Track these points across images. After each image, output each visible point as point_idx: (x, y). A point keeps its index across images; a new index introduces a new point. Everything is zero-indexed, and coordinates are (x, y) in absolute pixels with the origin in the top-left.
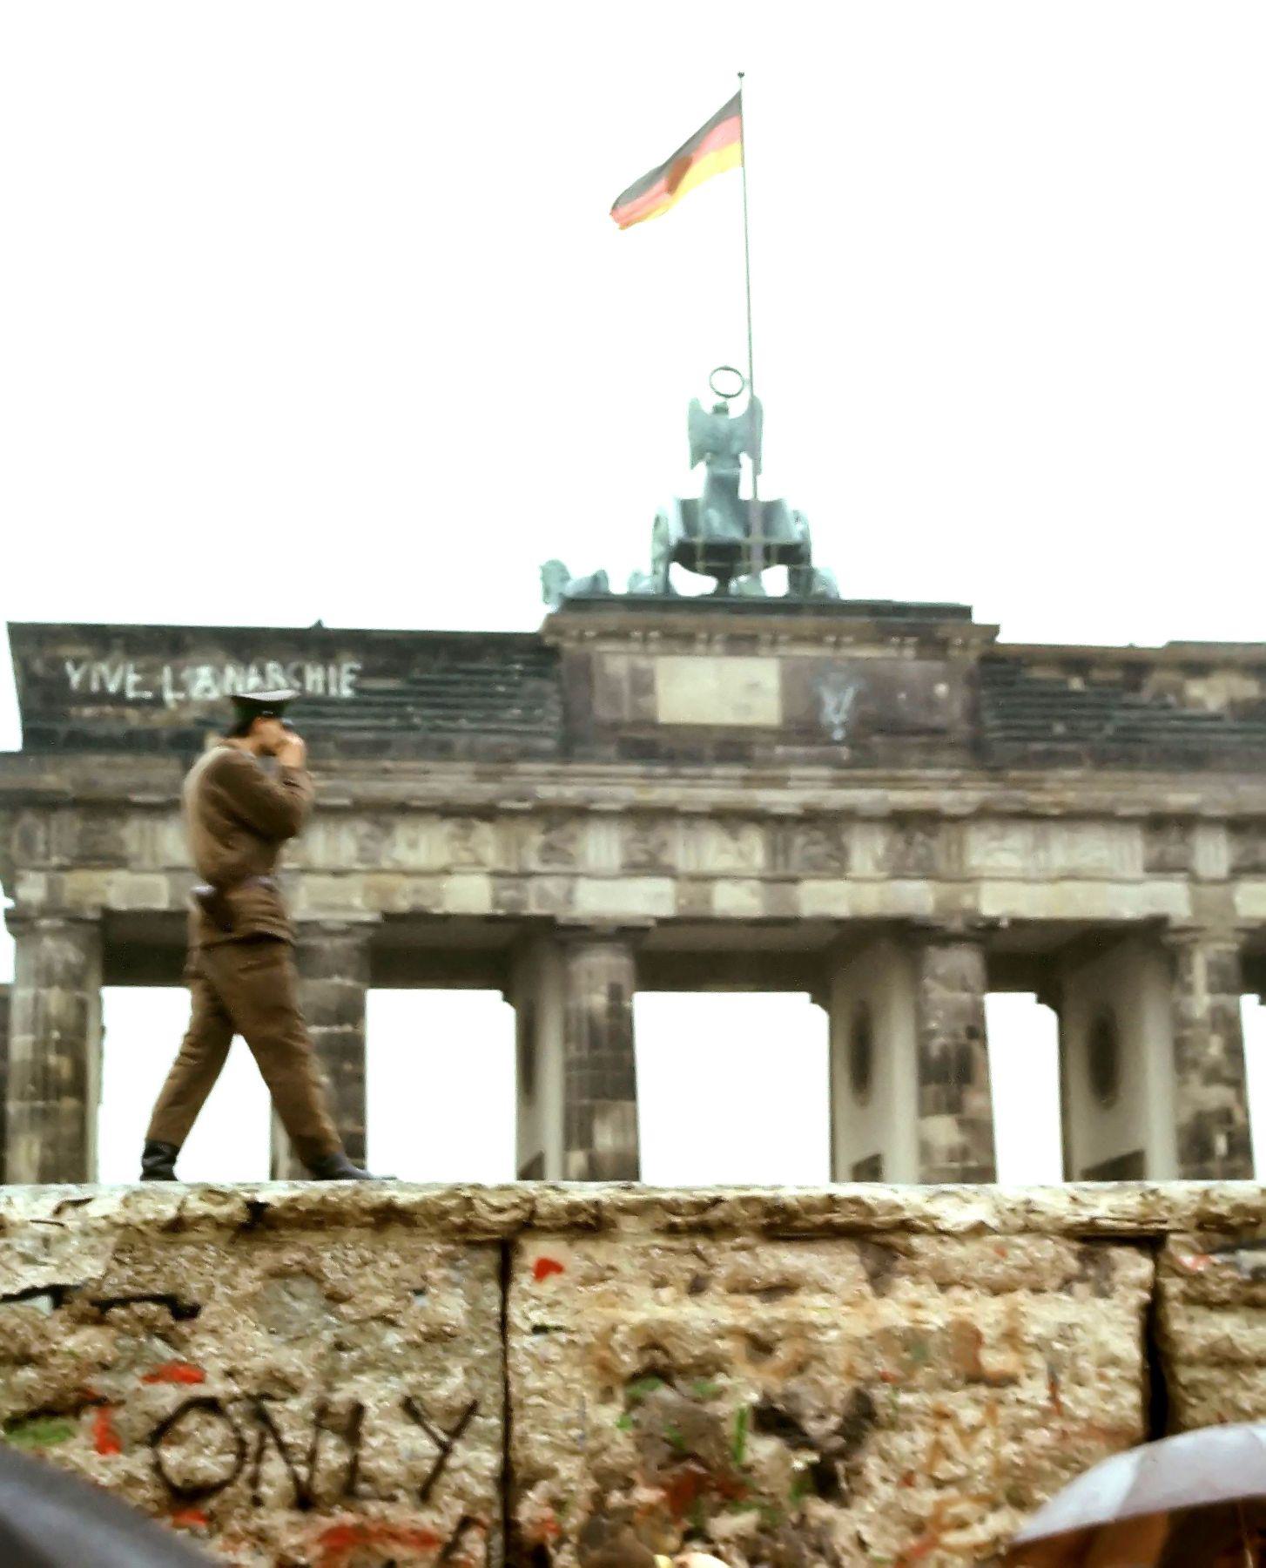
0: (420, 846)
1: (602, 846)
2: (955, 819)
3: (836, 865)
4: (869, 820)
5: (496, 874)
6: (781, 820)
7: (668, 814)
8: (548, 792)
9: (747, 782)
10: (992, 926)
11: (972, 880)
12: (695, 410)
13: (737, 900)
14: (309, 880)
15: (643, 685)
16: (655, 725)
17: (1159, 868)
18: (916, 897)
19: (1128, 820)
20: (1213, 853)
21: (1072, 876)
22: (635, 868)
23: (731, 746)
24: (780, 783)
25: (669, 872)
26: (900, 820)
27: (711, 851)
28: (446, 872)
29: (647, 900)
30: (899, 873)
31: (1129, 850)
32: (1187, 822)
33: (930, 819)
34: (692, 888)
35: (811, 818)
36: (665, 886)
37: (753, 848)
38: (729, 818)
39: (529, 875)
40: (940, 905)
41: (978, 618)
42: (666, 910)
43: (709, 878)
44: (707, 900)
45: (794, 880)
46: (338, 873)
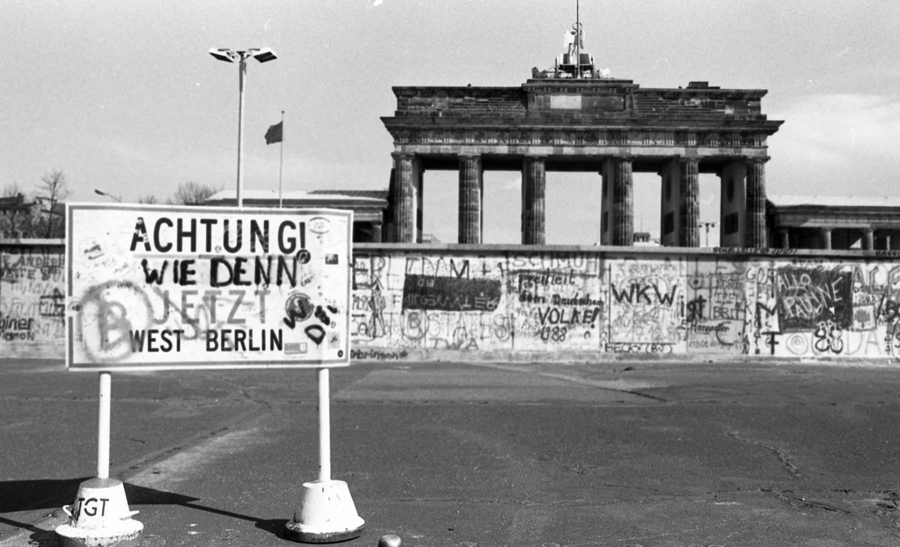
2: (624, 132)
4: (602, 132)
6: (580, 132)
7: (552, 130)
13: (568, 151)
14: (463, 147)
16: (549, 109)
18: (614, 151)
19: (670, 132)
22: (542, 145)
23: (569, 115)
26: (610, 132)
28: (497, 144)
29: (547, 151)
32: (686, 132)
34: (559, 148)
35: (587, 131)
36: (551, 148)
39: (517, 145)
40: (620, 152)
42: (551, 153)
44: (562, 151)
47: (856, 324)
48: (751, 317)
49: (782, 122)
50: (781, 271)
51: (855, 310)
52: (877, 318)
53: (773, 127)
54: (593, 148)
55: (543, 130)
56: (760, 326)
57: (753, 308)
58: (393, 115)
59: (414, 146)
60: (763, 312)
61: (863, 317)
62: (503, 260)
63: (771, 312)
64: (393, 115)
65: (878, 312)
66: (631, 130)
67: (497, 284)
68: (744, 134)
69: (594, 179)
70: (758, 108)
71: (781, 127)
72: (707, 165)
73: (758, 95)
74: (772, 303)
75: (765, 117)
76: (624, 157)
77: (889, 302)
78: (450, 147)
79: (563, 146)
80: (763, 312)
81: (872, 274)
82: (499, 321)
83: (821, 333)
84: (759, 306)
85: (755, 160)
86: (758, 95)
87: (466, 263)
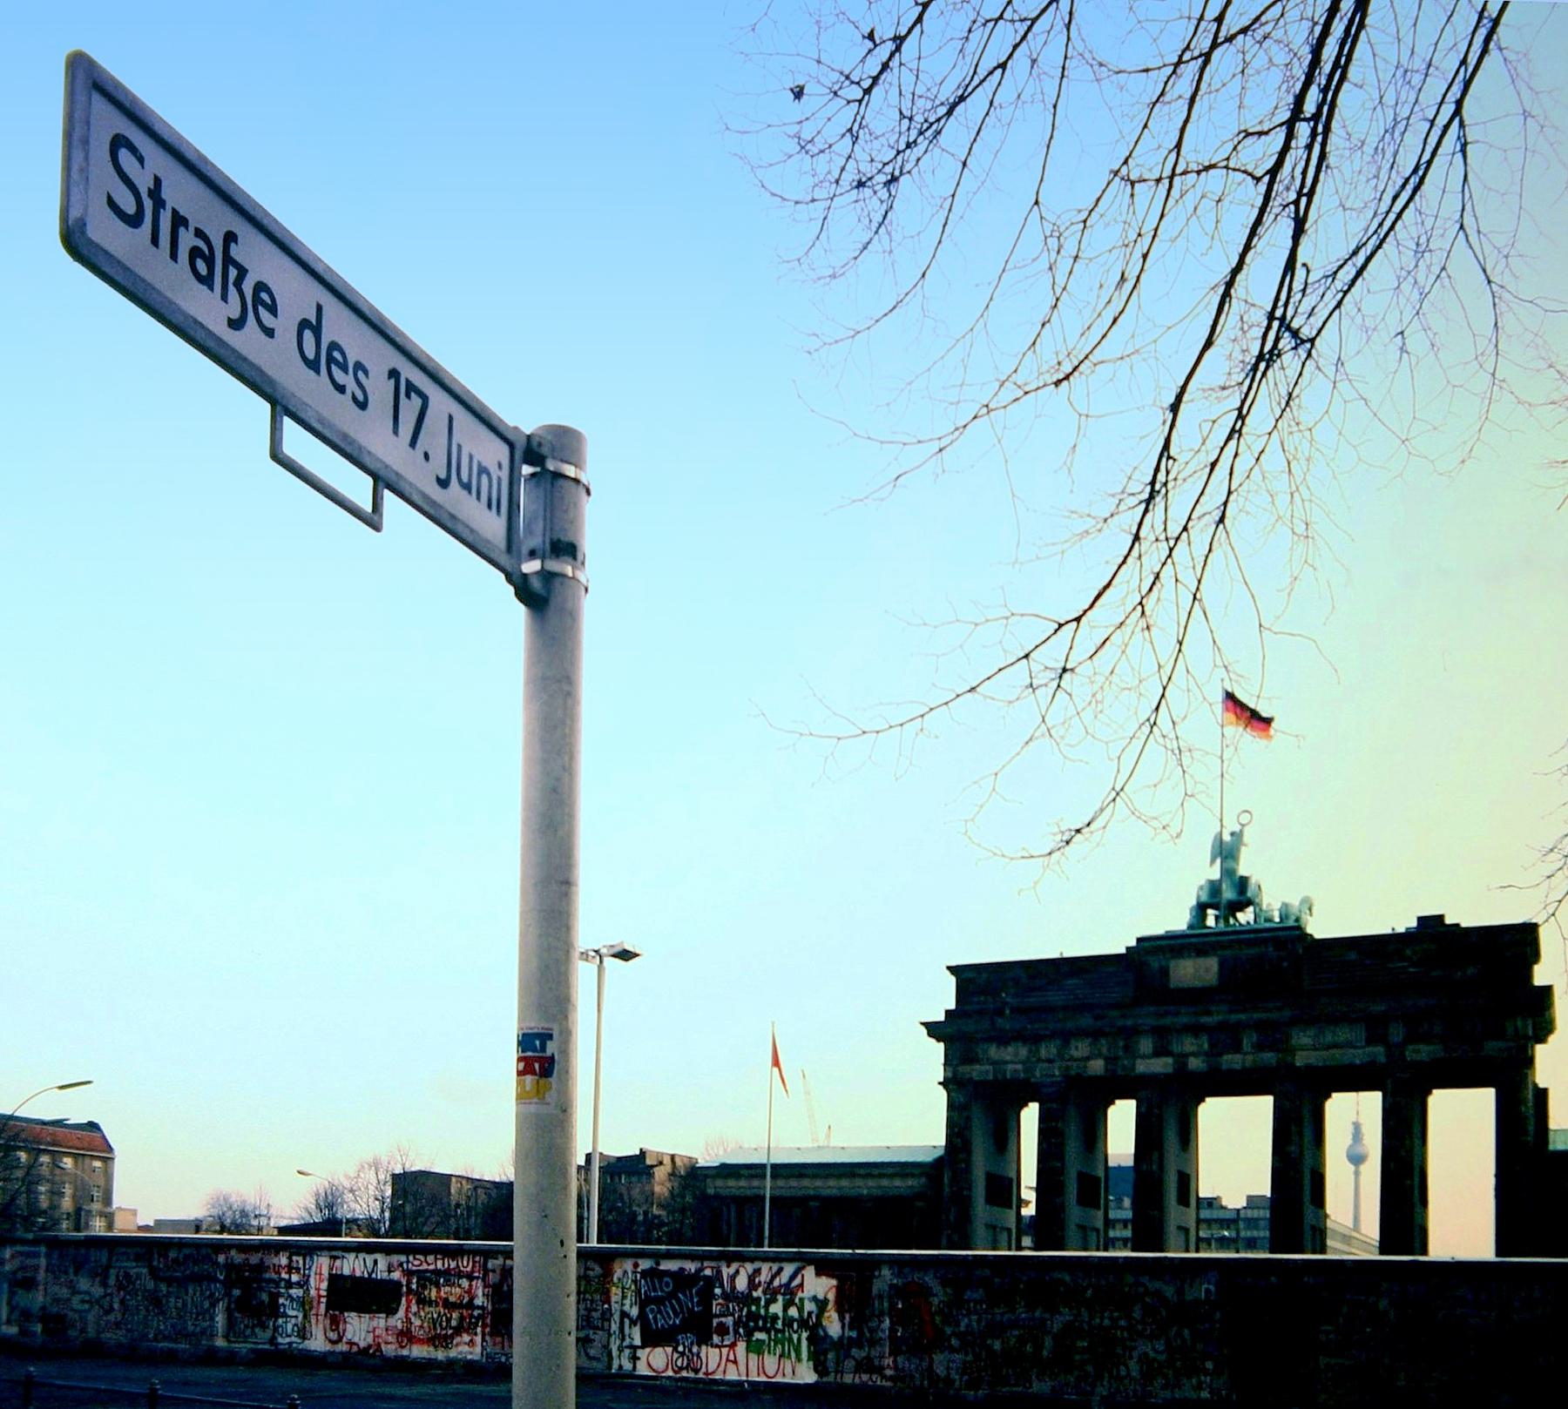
0: (1080, 1048)
1: (1146, 1045)
3: (1237, 1048)
5: (1106, 1059)
8: (1120, 1023)
9: (1196, 1014)
11: (1292, 1051)
13: (1195, 1063)
15: (1165, 972)
17: (1370, 1041)
18: (1269, 1057)
20: (1397, 1033)
21: (1336, 1046)
24: (1209, 1013)
25: (1168, 1053)
27: (1188, 1044)
28: (1088, 1058)
30: (1260, 1047)
35: (1222, 1026)
36: (1170, 1060)
38: (1195, 1030)
43: (1186, 1056)
44: (1185, 1064)
45: (1221, 1055)
46: (1050, 1061)
47: (716, 1339)
48: (614, 1327)
50: (644, 1274)
51: (715, 1322)
52: (736, 1332)
54: (1238, 1057)
56: (623, 1339)
57: (617, 1317)
58: (942, 1018)
59: (967, 1068)
60: (627, 1321)
61: (722, 1329)
62: (403, 1258)
63: (633, 1323)
64: (942, 1018)
65: (737, 1324)
67: (398, 1284)
74: (635, 1312)
77: (749, 1311)
78: (1019, 1067)
80: (627, 1321)
81: (733, 1278)
82: (399, 1325)
83: (681, 1349)
84: (624, 1315)
87: (376, 1262)
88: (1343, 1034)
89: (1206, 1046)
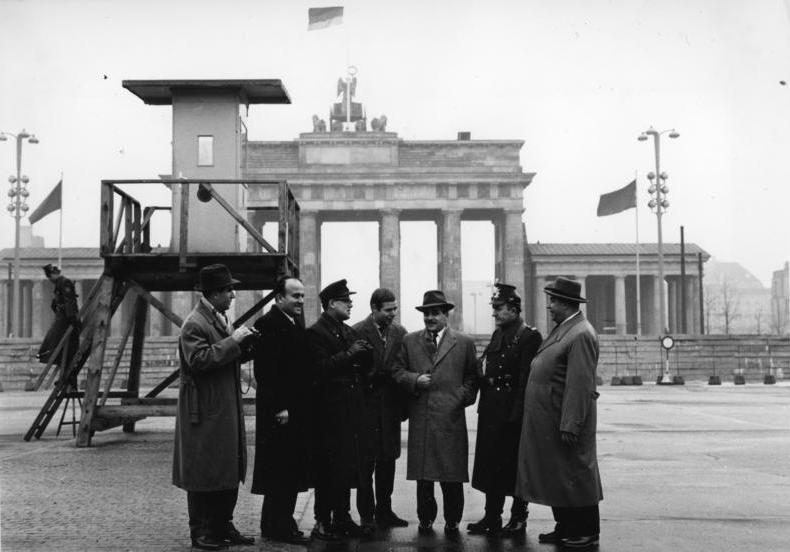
2: (390, 186)
3: (361, 196)
4: (370, 187)
6: (349, 187)
10: (397, 211)
12: (340, 80)
13: (339, 206)
17: (440, 196)
18: (379, 205)
20: (453, 193)
26: (376, 186)
31: (433, 193)
33: (384, 186)
37: (343, 193)
41: (399, 136)
49: (533, 175)
53: (525, 181)
55: (313, 186)
66: (396, 184)
68: (501, 186)
69: (373, 227)
70: (517, 158)
71: (534, 179)
72: (471, 215)
73: (518, 145)
75: (520, 169)
76: (389, 210)
79: (332, 201)
85: (511, 212)
86: (518, 145)
88: (423, 193)
89: (344, 196)
